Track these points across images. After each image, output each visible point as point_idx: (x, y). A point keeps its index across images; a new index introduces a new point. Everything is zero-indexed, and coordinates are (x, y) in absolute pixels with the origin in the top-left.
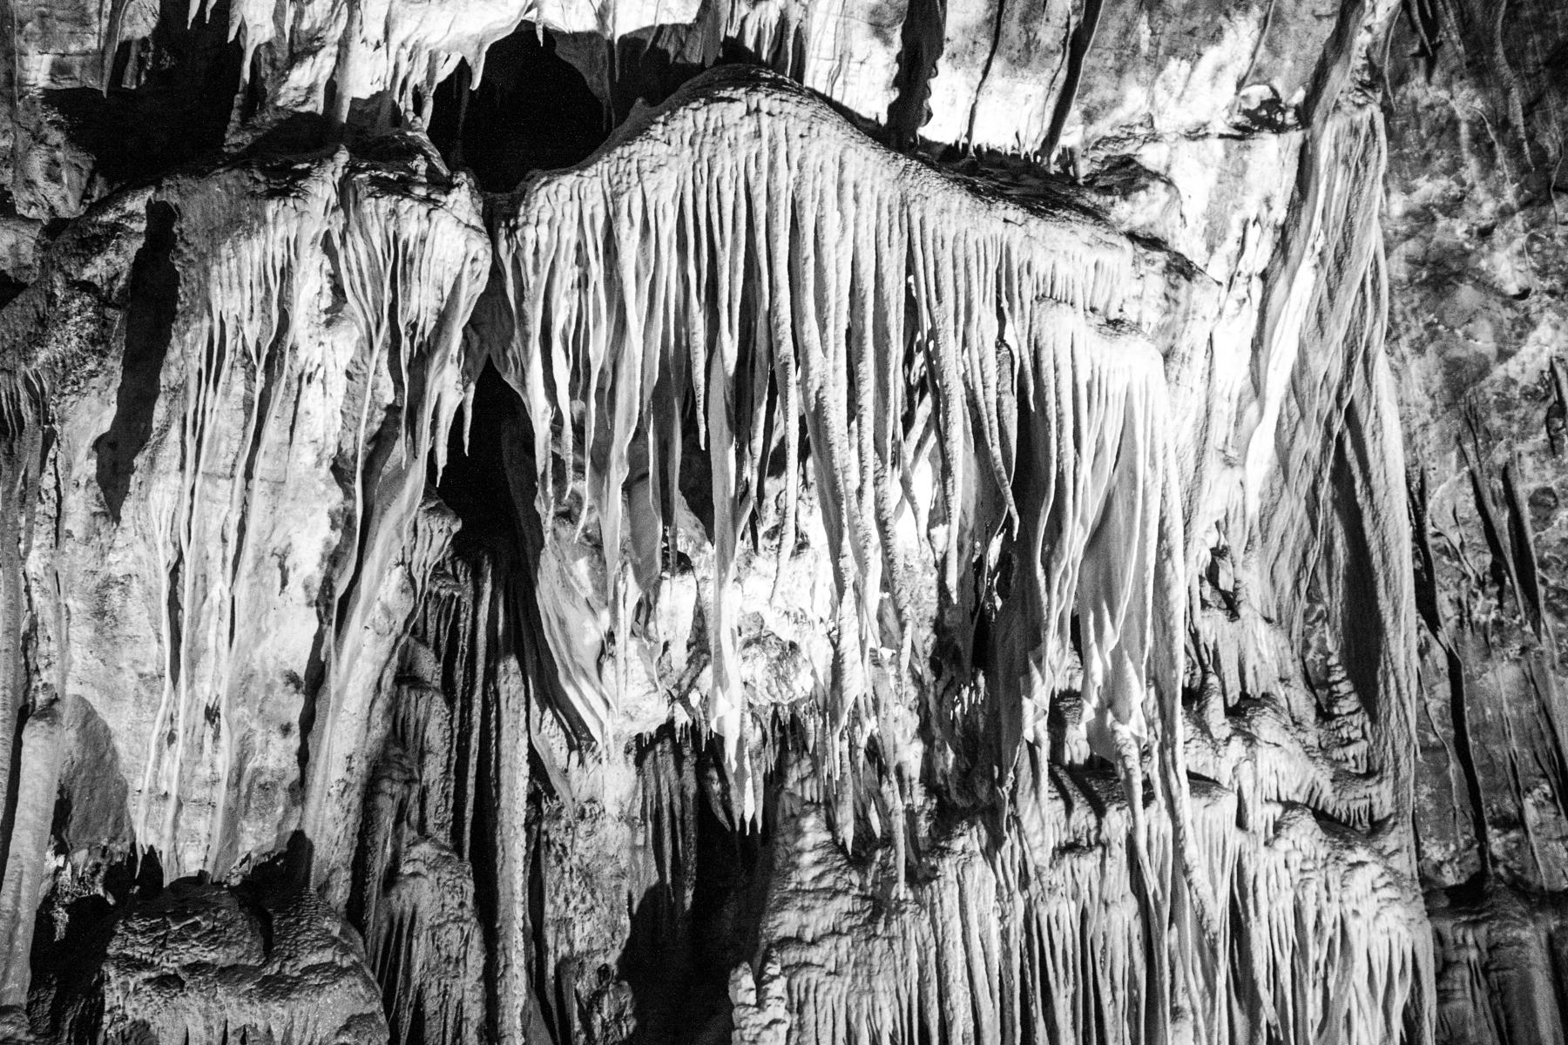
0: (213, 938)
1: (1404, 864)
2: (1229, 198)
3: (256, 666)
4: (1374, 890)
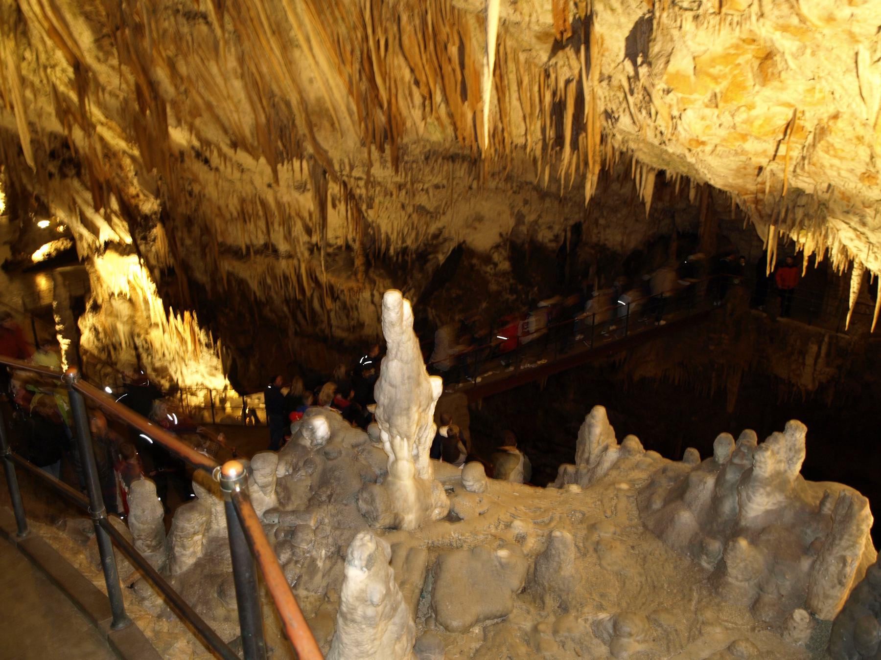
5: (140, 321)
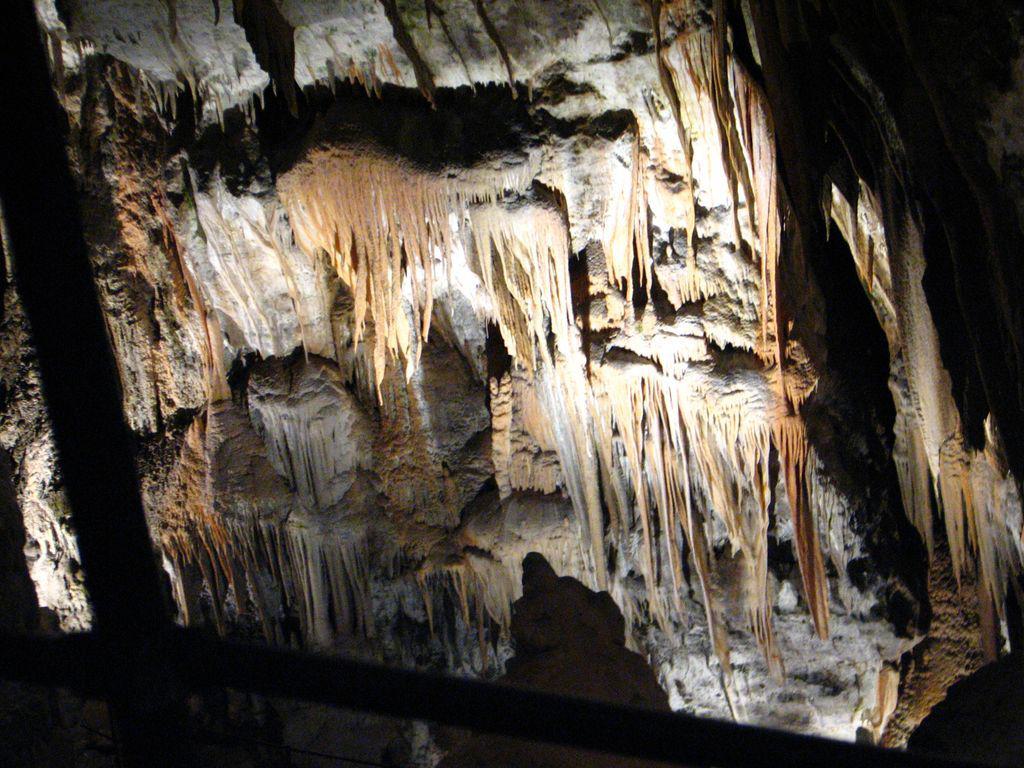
0: (273, 386)
1: (778, 389)
4: (747, 402)
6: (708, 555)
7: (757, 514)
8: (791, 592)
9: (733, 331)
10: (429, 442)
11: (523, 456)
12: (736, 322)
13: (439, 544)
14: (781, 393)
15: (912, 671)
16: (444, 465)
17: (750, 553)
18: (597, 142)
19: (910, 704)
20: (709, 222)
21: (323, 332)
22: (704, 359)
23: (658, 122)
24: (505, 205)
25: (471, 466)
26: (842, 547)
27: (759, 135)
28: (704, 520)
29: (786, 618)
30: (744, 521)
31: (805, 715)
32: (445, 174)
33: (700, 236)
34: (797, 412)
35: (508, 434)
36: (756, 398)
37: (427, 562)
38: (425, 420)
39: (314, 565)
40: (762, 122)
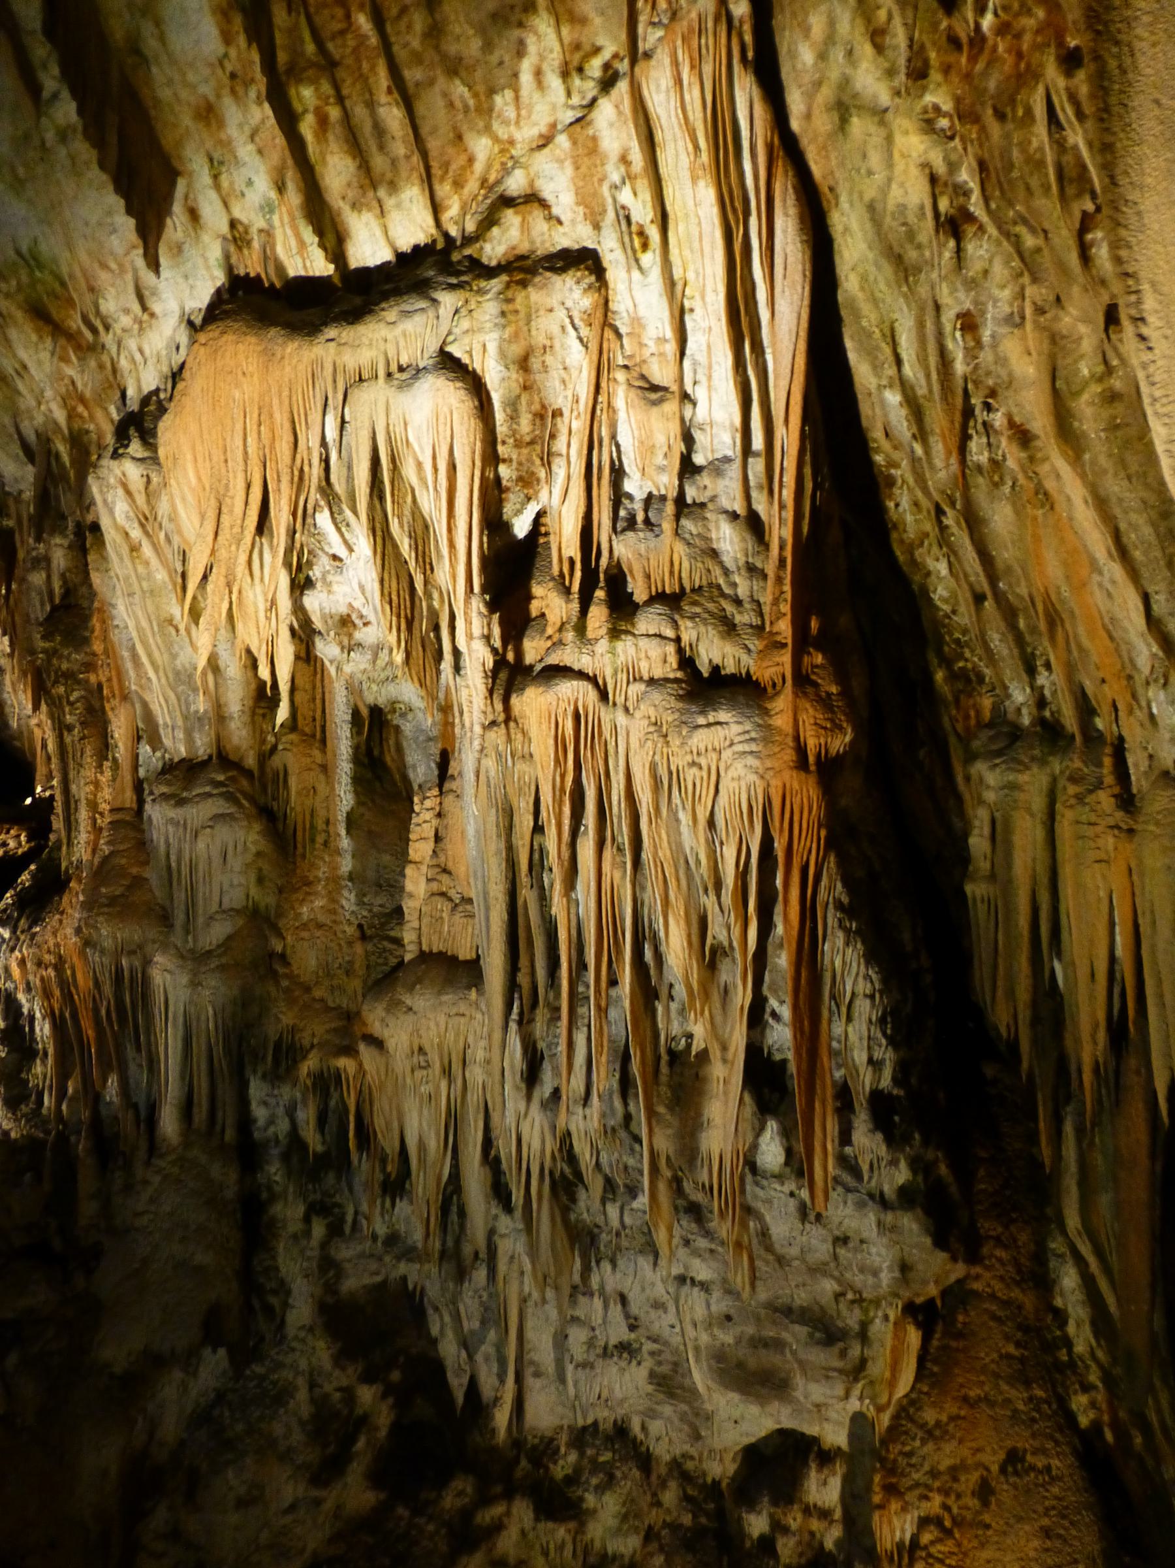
2: (592, 175)
3: (179, 667)
4: (731, 745)
5: (307, 959)
6: (658, 1058)
7: (735, 987)
8: (777, 1139)
9: (723, 638)
10: (345, 893)
11: (440, 903)
12: (729, 628)
13: (335, 1030)
14: (789, 729)
15: (937, 1336)
16: (360, 926)
17: (718, 1053)
18: (537, 279)
19: (932, 1386)
20: (705, 479)
21: (244, 732)
22: (672, 676)
23: (636, 274)
24: (396, 382)
25: (392, 933)
26: (865, 1057)
27: (785, 231)
28: (657, 997)
29: (765, 1183)
30: (716, 997)
31: (783, 1375)
32: (322, 338)
33: (689, 501)
34: (813, 768)
35: (424, 868)
36: (747, 737)
37: (315, 1051)
38: (346, 865)
39: (175, 1025)
40: (793, 211)
